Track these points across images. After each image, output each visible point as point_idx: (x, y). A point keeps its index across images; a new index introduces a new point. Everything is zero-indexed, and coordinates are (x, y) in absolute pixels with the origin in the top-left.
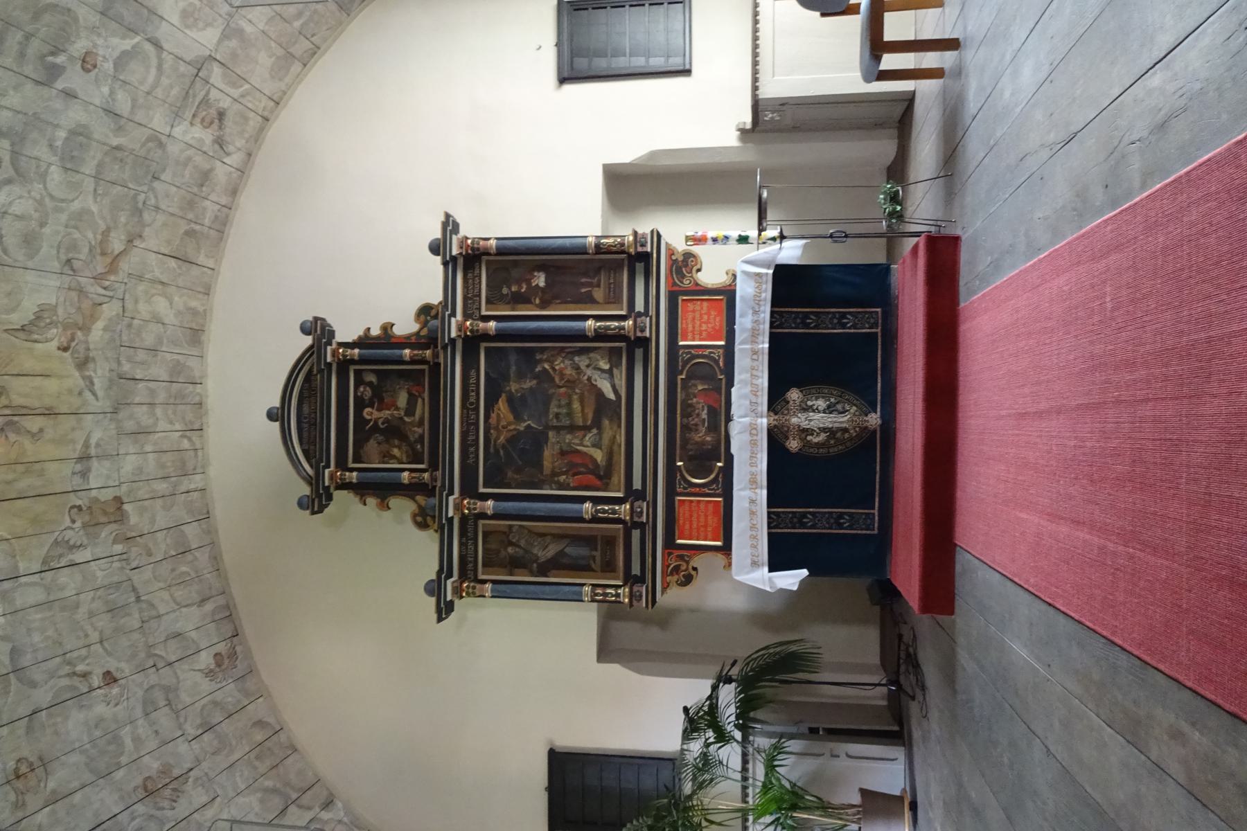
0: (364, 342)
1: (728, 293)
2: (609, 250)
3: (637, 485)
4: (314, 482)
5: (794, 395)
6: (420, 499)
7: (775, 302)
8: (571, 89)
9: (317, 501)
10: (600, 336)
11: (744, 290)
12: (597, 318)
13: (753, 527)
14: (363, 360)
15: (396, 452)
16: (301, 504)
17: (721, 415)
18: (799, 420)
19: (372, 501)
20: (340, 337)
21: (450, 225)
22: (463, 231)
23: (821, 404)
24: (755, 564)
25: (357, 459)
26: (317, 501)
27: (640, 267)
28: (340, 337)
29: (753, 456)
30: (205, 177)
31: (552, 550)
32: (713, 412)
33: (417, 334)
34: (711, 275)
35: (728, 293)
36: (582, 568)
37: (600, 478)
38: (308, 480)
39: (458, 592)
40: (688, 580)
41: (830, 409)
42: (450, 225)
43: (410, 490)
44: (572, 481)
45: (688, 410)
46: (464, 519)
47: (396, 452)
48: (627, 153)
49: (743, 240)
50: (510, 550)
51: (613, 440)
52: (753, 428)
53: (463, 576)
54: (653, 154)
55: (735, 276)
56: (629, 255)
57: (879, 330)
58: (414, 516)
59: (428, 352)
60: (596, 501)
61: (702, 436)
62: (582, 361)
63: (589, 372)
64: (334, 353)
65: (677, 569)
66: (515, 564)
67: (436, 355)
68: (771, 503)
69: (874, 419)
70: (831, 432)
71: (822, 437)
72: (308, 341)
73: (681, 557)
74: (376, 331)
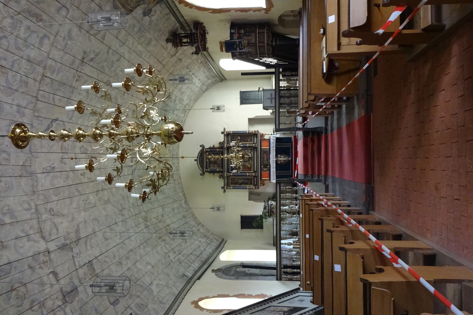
0: (210, 148)
1: (269, 140)
2: (250, 133)
3: (255, 170)
4: (203, 171)
5: (279, 155)
6: (220, 174)
7: (276, 142)
8: (242, 105)
9: (203, 174)
10: (249, 147)
11: (272, 141)
12: (249, 144)
13: (274, 174)
14: (210, 151)
15: (216, 166)
16: (201, 175)
17: (269, 159)
18: (280, 159)
19: (212, 174)
20: (206, 147)
21: (224, 129)
22: (226, 130)
23: (283, 157)
24: (274, 179)
25: (209, 167)
26: (203, 174)
28: (206, 147)
29: (273, 164)
30: (182, 121)
31: (242, 181)
32: (267, 159)
33: (219, 147)
34: (266, 137)
35: (269, 140)
36: (247, 184)
37: (249, 169)
38: (202, 171)
39: (227, 188)
40: (264, 185)
41: (284, 157)
42: (224, 129)
44: (245, 170)
45: (263, 158)
46: (227, 176)
47: (216, 166)
48: (252, 117)
49: (271, 134)
50: (235, 181)
51: (251, 163)
52: (273, 160)
53: (227, 186)
55: (270, 137)
56: (254, 134)
57: (290, 146)
58: (219, 176)
59: (221, 150)
60: (249, 173)
61: (266, 162)
62: (246, 151)
63: (247, 153)
64: (205, 150)
65: (262, 183)
66: (236, 184)
67: (222, 150)
68: (276, 171)
69: (290, 159)
70: (284, 161)
71: (283, 161)
72: (201, 148)
73: (263, 181)
74: (212, 146)
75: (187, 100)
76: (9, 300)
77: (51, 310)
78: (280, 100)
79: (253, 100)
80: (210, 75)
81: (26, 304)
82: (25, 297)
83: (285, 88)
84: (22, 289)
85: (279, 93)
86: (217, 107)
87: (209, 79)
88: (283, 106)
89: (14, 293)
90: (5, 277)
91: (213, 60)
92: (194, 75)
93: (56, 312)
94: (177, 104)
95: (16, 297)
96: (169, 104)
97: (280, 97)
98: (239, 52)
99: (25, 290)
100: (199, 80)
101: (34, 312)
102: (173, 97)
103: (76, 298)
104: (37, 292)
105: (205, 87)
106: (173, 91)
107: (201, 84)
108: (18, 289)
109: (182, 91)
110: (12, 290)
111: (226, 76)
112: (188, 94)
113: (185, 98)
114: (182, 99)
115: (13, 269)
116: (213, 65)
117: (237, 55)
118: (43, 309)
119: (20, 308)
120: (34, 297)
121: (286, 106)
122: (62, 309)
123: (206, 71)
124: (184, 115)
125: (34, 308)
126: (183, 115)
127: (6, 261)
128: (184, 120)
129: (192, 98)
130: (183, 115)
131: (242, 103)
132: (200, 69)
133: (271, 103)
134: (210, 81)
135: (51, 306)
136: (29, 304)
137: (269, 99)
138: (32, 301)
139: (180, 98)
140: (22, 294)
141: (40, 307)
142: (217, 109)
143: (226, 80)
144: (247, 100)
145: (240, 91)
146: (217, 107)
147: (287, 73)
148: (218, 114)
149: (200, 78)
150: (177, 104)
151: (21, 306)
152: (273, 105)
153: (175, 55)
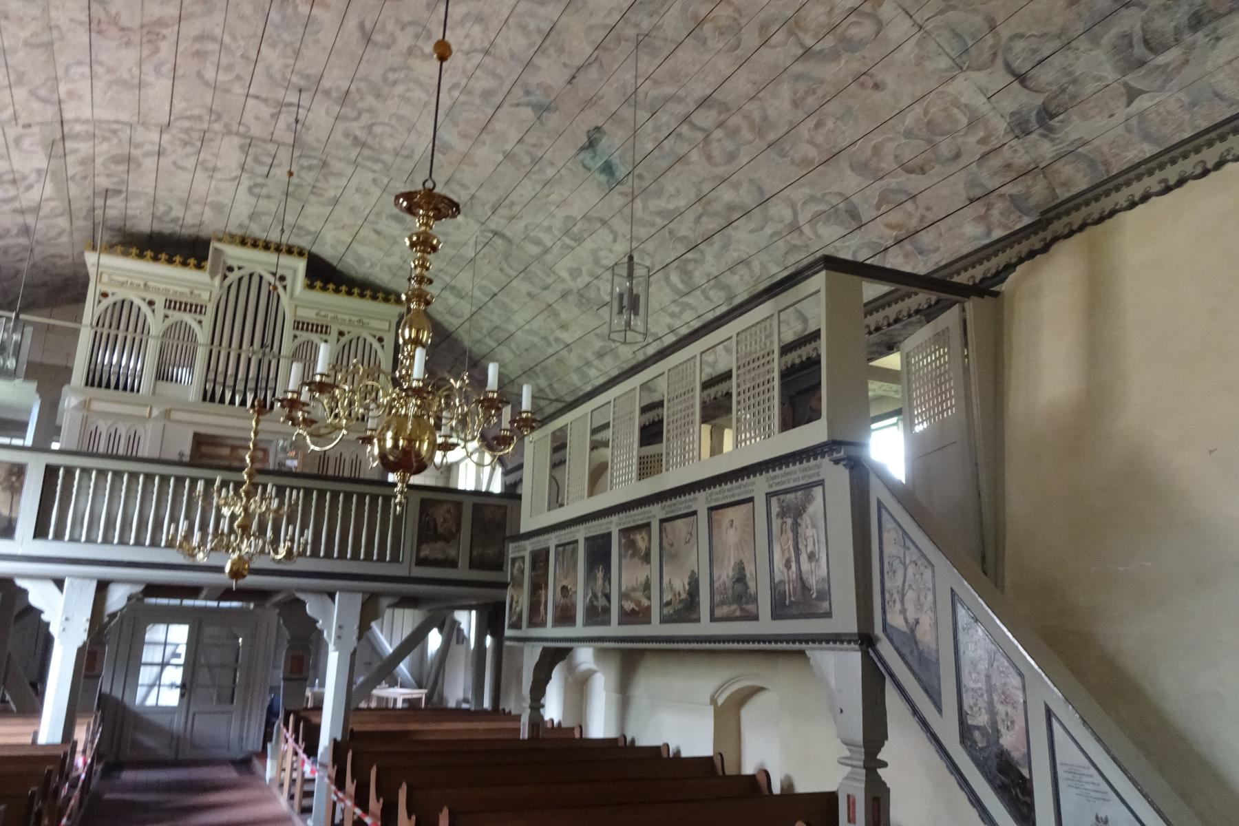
76: (705, 43)
77: (825, 31)
81: (751, 39)
82: (739, 24)
89: (707, 27)
93: (846, 30)
95: (717, 33)
99: (731, 9)
101: (778, 49)
110: (700, 23)
118: (801, 35)
120: (762, 15)
122: (868, 15)
125: (774, 40)
135: (823, 19)
136: (757, 34)
141: (791, 33)
151: (738, 47)
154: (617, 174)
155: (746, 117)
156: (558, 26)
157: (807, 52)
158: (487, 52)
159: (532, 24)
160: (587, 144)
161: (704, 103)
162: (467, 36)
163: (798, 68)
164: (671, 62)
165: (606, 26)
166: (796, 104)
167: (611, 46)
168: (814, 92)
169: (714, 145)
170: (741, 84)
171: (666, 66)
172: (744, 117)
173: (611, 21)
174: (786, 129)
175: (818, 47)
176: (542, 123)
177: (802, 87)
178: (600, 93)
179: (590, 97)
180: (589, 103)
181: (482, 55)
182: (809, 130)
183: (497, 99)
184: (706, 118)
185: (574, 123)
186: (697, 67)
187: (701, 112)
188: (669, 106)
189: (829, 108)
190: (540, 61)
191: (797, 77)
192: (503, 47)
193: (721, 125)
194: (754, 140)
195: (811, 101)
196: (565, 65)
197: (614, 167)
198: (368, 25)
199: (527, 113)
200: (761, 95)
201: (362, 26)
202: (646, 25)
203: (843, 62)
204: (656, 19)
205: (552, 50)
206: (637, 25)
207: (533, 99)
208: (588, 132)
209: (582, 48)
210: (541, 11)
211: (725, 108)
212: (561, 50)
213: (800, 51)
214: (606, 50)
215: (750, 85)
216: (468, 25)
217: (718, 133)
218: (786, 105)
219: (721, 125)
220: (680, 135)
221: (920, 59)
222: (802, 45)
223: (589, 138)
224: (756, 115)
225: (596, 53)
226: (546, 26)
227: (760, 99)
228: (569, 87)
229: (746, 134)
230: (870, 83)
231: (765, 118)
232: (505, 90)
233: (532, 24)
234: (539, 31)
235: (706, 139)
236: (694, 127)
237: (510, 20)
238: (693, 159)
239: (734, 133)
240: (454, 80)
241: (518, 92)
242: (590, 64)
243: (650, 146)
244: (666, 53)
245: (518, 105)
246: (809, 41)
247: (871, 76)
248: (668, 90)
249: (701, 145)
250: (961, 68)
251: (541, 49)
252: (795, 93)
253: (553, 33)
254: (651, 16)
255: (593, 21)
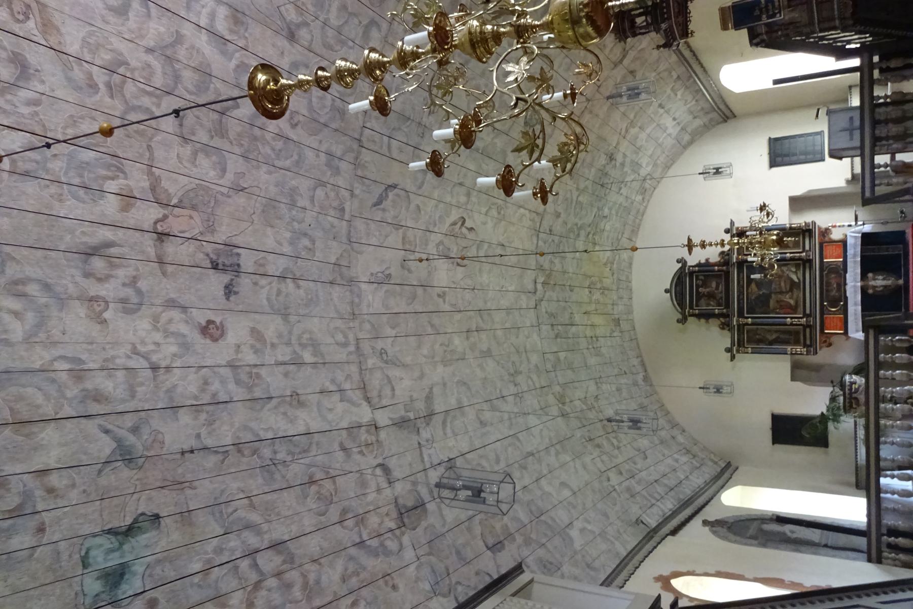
0: (699, 265)
1: (844, 242)
2: (794, 229)
3: (808, 312)
4: (683, 314)
5: (870, 275)
6: (722, 320)
7: (862, 245)
8: (775, 169)
9: (683, 320)
10: (792, 259)
11: (850, 241)
12: (791, 253)
13: (856, 319)
14: (699, 271)
15: (712, 303)
16: (678, 321)
17: (842, 285)
18: (872, 283)
19: (703, 321)
20: (689, 264)
21: (732, 223)
22: (736, 225)
23: (881, 277)
24: (857, 331)
25: (697, 306)
26: (683, 320)
27: (807, 234)
28: (689, 264)
29: (855, 295)
30: (639, 210)
31: (774, 336)
32: (839, 285)
33: (719, 261)
34: (836, 235)
35: (844, 242)
36: (787, 342)
37: (792, 309)
38: (681, 313)
39: (738, 351)
40: (830, 345)
41: (884, 279)
42: (732, 223)
43: (721, 315)
44: (782, 311)
45: (829, 284)
46: (739, 325)
47: (712, 303)
48: (798, 192)
49: (850, 226)
50: (757, 337)
51: (798, 297)
52: (855, 286)
53: (739, 345)
54: (810, 191)
55: (846, 236)
56: (803, 230)
57: (902, 252)
58: (719, 325)
59: (724, 268)
60: (792, 318)
61: (834, 293)
62: (785, 269)
63: (787, 272)
64: (689, 269)
65: (825, 341)
66: (759, 341)
67: (727, 268)
68: (863, 310)
69: (901, 282)
70: (885, 287)
71: (881, 288)
72: (680, 265)
73: (827, 337)
74: (703, 261)
75: (648, 164)
76: (306, 498)
77: (375, 534)
78: (873, 128)
79: (801, 154)
80: (699, 108)
81: (334, 514)
83: (888, 100)
84: (328, 485)
85: (872, 112)
86: (714, 169)
87: (695, 118)
88: (884, 142)
89: (314, 488)
90: (300, 456)
91: (705, 71)
92: (663, 108)
94: (627, 172)
96: (609, 173)
97: (875, 123)
98: (767, 25)
100: (674, 119)
101: (346, 531)
102: (619, 158)
103: (423, 523)
104: (353, 495)
105: (687, 138)
106: (618, 143)
107: (679, 128)
108: (321, 482)
109: (638, 145)
110: (312, 482)
111: (736, 107)
112: (650, 152)
113: (644, 161)
114: (637, 163)
115: (314, 447)
116: (705, 82)
117: (761, 34)
119: (323, 518)
120: (347, 503)
121: (891, 142)
122: (397, 537)
123: (689, 97)
124: (643, 199)
125: (346, 523)
126: (639, 198)
127: (302, 429)
128: (642, 208)
129: (659, 162)
130: (639, 198)
131: (773, 163)
132: (676, 95)
133: (851, 139)
134: (698, 122)
135: (376, 526)
136: (339, 513)
137: (845, 130)
138: (344, 510)
139: (632, 161)
140: (328, 494)
142: (715, 174)
143: (735, 116)
144: (787, 155)
145: (770, 138)
146: (714, 169)
147: (893, 64)
148: (717, 183)
149: (677, 115)
150: (627, 172)
152: (857, 143)
153: (621, 61)
154: (124, 586)
155: (304, 576)
156: (229, 406)
157: (361, 544)
158: (155, 368)
159: (216, 386)
160: (124, 529)
161: (276, 546)
162: (157, 344)
163: (353, 551)
164: (275, 496)
165: (258, 435)
166: (344, 580)
167: (246, 453)
168: (358, 574)
169: (263, 593)
170: (314, 544)
171: (269, 497)
172: (302, 574)
173: (263, 435)
174: (329, 599)
175: (368, 543)
176: (100, 471)
177: (351, 567)
178: (196, 484)
179: (183, 480)
180: (179, 485)
181: (148, 366)
182: (347, 606)
183: (95, 408)
184: (269, 562)
185: (135, 496)
186: (290, 513)
187: (270, 553)
188: (246, 534)
189: (364, 592)
190: (185, 417)
191: (351, 558)
192: (175, 377)
193: (278, 575)
194: (301, 601)
195: (354, 582)
196: (198, 436)
197: (126, 577)
198: (113, 251)
199: (105, 447)
200: (322, 561)
201: (110, 244)
202: (280, 456)
203: (380, 560)
204: (289, 458)
205: (203, 416)
206: (275, 452)
207: (131, 439)
208: (143, 514)
209: (225, 435)
210: (232, 386)
211: (290, 559)
212: (210, 423)
213: (358, 540)
214: (239, 451)
215: (318, 548)
216: (171, 340)
217: (272, 582)
218: (336, 576)
219: (278, 575)
220: (236, 568)
221: (418, 579)
222: (361, 537)
223: (136, 521)
224: (312, 577)
225: (232, 447)
226: (223, 397)
227: (320, 564)
228: (179, 456)
229: (297, 593)
230: (391, 583)
231: (318, 582)
232: (121, 408)
233: (216, 386)
234: (214, 395)
235: (257, 586)
236: (255, 566)
237: (205, 370)
238: (231, 603)
239: (289, 586)
240: (83, 357)
241: (129, 421)
242: (217, 452)
243: (197, 566)
244: (276, 487)
245: (107, 432)
246: (365, 537)
247: (392, 578)
248: (255, 517)
249: (249, 589)
250: (435, 593)
251: (199, 408)
252: (346, 570)
253: (221, 406)
254: (288, 454)
255: (253, 425)
